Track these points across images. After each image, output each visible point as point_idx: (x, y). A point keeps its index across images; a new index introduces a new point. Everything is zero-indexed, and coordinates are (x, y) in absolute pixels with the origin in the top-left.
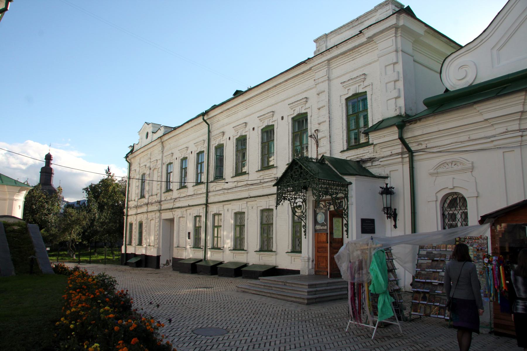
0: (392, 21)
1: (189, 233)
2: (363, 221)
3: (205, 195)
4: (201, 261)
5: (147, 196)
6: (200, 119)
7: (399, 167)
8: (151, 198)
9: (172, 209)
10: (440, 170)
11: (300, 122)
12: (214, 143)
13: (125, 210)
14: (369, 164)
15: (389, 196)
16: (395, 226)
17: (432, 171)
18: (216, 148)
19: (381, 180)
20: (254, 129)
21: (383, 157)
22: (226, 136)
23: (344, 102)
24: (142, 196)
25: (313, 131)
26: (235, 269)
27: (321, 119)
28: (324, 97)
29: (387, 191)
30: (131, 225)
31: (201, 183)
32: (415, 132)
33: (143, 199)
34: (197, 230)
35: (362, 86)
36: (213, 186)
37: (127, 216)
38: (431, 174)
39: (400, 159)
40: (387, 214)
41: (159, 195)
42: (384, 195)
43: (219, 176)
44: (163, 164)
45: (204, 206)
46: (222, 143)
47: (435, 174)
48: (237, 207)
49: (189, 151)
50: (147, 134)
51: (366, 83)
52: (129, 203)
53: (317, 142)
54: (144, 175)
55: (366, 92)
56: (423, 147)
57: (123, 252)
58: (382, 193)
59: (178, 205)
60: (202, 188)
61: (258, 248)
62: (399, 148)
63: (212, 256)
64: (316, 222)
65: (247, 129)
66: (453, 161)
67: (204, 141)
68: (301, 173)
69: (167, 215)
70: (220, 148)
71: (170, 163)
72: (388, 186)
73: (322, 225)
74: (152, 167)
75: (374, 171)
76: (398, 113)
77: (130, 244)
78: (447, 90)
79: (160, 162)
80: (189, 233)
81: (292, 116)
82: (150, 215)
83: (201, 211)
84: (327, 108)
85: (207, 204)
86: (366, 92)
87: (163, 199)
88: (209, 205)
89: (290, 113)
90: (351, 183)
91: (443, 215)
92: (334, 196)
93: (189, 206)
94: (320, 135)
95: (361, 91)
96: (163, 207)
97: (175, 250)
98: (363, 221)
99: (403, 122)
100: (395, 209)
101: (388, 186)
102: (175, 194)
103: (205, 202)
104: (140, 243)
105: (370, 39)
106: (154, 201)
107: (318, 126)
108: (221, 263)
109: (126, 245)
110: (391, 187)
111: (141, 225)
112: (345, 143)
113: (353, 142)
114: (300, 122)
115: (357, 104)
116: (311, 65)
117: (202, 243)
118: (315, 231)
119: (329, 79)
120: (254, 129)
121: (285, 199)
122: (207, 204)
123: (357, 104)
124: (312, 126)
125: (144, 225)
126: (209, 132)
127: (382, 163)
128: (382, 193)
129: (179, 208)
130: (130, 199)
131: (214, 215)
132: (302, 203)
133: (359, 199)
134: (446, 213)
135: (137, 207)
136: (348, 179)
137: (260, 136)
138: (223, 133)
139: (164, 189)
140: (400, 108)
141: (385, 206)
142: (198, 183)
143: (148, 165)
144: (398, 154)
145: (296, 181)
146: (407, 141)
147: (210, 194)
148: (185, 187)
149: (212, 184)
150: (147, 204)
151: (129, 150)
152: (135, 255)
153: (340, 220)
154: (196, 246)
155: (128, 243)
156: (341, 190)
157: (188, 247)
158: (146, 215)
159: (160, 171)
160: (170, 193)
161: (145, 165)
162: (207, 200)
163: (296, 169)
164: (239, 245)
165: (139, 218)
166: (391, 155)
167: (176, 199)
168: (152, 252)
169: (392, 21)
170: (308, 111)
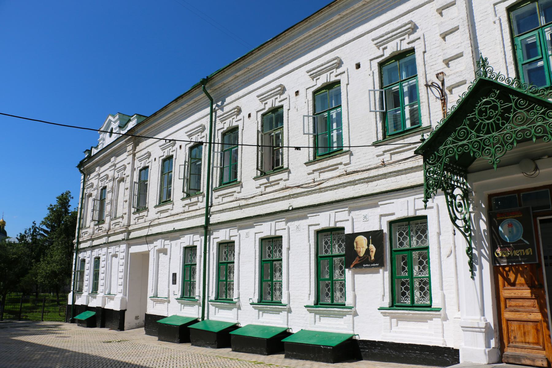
1: (174, 275)
4: (196, 321)
34: (189, 269)
41: (126, 217)
43: (230, 178)
44: (133, 169)
48: (266, 229)
57: (70, 302)
74: (116, 176)
79: (129, 168)
80: (174, 275)
81: (380, 60)
82: (112, 250)
93: (175, 231)
97: (150, 302)
102: (152, 213)
103: (204, 223)
108: (235, 327)
109: (74, 293)
117: (198, 291)
131: (220, 244)
132: (463, 199)
152: (85, 308)
154: (187, 294)
157: (172, 298)
158: (104, 250)
162: (207, 220)
165: (96, 253)
168: (114, 305)
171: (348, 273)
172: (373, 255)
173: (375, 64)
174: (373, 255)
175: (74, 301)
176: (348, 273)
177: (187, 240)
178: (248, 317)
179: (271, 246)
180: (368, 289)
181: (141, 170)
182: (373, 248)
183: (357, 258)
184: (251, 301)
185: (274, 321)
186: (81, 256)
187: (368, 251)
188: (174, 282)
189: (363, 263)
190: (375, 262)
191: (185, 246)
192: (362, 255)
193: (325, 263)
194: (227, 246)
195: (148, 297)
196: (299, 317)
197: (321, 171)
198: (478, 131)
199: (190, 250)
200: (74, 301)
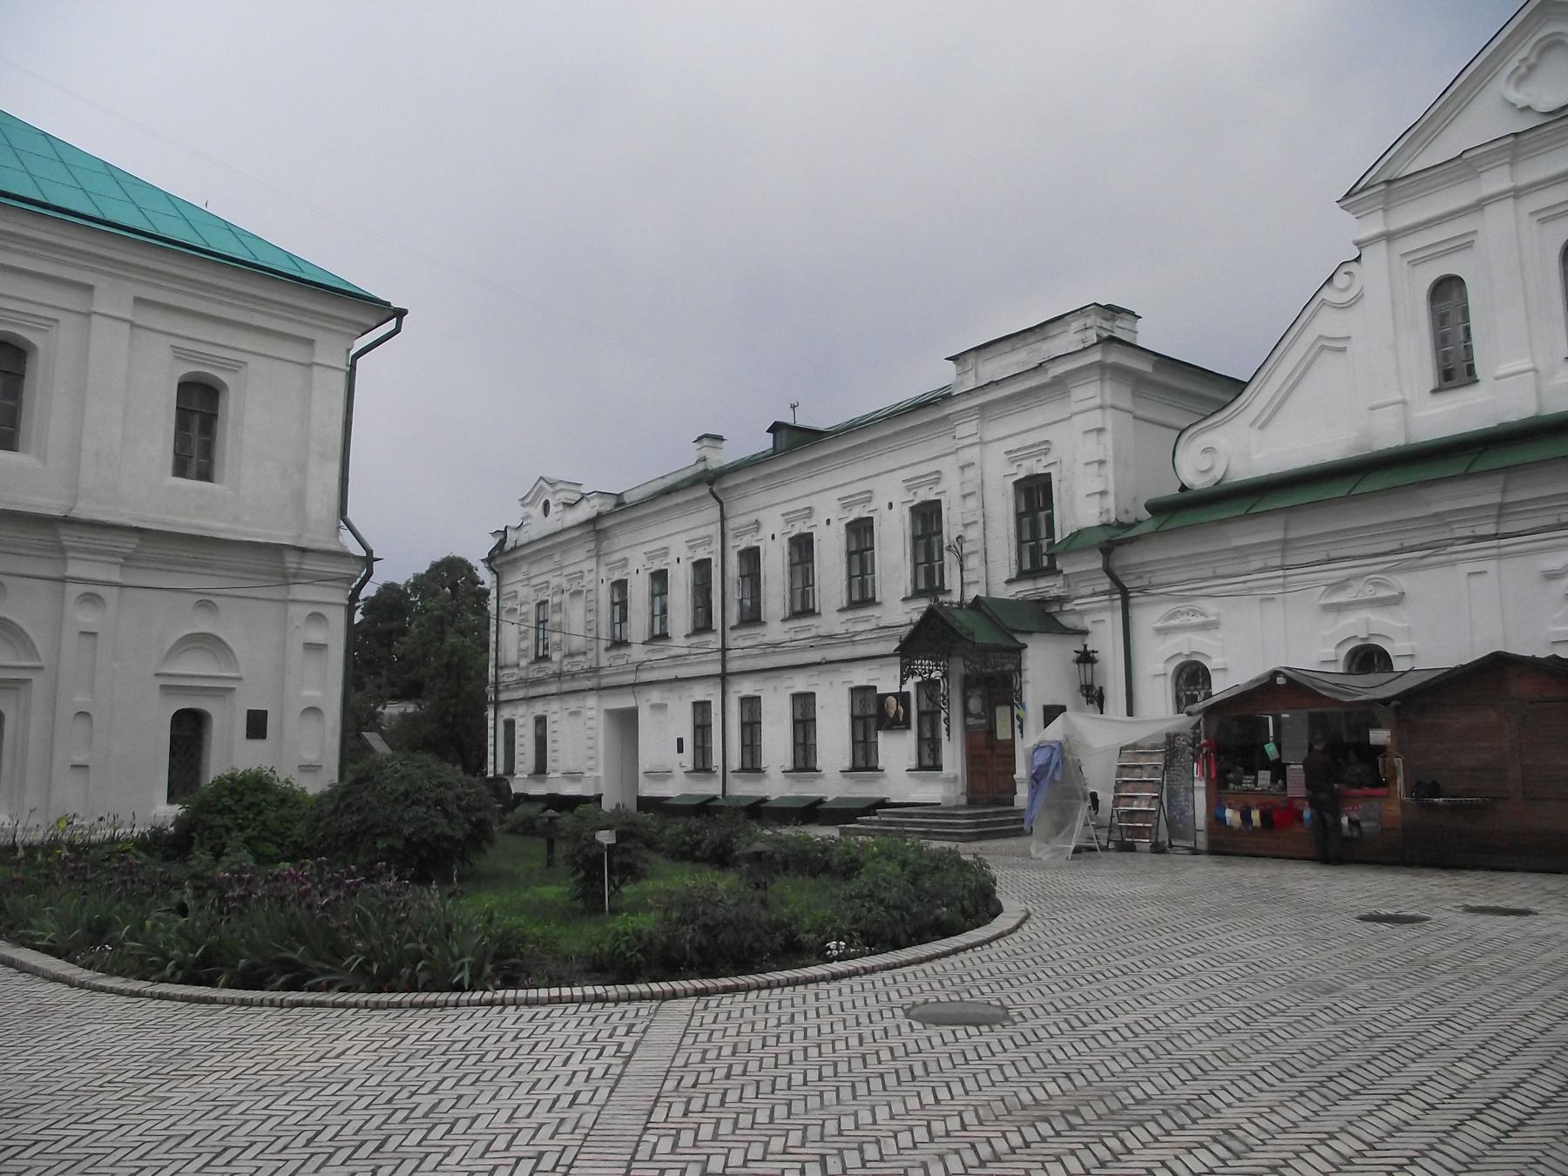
0: (1096, 356)
1: (680, 741)
3: (718, 656)
4: (714, 798)
5: (556, 656)
6: (704, 490)
7: (1106, 616)
8: (566, 662)
9: (634, 685)
10: (1173, 622)
11: (927, 517)
13: (490, 689)
14: (1055, 608)
17: (1158, 625)
18: (742, 554)
19: (1077, 638)
20: (828, 522)
23: (1011, 488)
25: (953, 538)
29: (1086, 658)
30: (510, 725)
32: (1130, 557)
34: (702, 729)
36: (737, 640)
40: (1087, 696)
43: (752, 617)
45: (719, 680)
47: (1163, 631)
48: (801, 683)
50: (547, 504)
52: (501, 673)
56: (1145, 582)
58: (1078, 661)
59: (646, 676)
61: (847, 764)
62: (1106, 584)
63: (744, 789)
64: (966, 713)
69: (623, 702)
70: (751, 557)
73: (978, 717)
75: (1066, 621)
76: (1105, 519)
78: (1183, 488)
80: (680, 741)
82: (573, 703)
84: (979, 494)
87: (604, 663)
88: (731, 678)
93: (677, 679)
95: (1041, 471)
96: (605, 682)
99: (1112, 541)
102: (637, 653)
104: (541, 769)
111: (541, 721)
112: (1014, 566)
114: (927, 517)
115: (1035, 495)
117: (716, 760)
118: (966, 728)
120: (828, 522)
123: (1035, 495)
124: (951, 525)
126: (723, 519)
128: (1078, 661)
129: (651, 683)
130: (502, 662)
131: (743, 700)
136: (1021, 639)
137: (844, 538)
140: (1108, 511)
143: (555, 582)
144: (1104, 593)
146: (1118, 573)
147: (730, 654)
149: (736, 633)
150: (559, 676)
151: (493, 542)
153: (1008, 709)
160: (623, 651)
164: (804, 759)
165: (539, 708)
166: (1094, 594)
167: (642, 663)
169: (1096, 356)
171: (881, 734)
173: (906, 508)
176: (881, 734)
177: (699, 693)
179: (804, 706)
180: (897, 750)
182: (901, 709)
186: (506, 713)
187: (897, 712)
188: (680, 750)
189: (898, 724)
193: (860, 724)
194: (751, 705)
195: (641, 775)
196: (833, 779)
197: (855, 621)
199: (702, 708)
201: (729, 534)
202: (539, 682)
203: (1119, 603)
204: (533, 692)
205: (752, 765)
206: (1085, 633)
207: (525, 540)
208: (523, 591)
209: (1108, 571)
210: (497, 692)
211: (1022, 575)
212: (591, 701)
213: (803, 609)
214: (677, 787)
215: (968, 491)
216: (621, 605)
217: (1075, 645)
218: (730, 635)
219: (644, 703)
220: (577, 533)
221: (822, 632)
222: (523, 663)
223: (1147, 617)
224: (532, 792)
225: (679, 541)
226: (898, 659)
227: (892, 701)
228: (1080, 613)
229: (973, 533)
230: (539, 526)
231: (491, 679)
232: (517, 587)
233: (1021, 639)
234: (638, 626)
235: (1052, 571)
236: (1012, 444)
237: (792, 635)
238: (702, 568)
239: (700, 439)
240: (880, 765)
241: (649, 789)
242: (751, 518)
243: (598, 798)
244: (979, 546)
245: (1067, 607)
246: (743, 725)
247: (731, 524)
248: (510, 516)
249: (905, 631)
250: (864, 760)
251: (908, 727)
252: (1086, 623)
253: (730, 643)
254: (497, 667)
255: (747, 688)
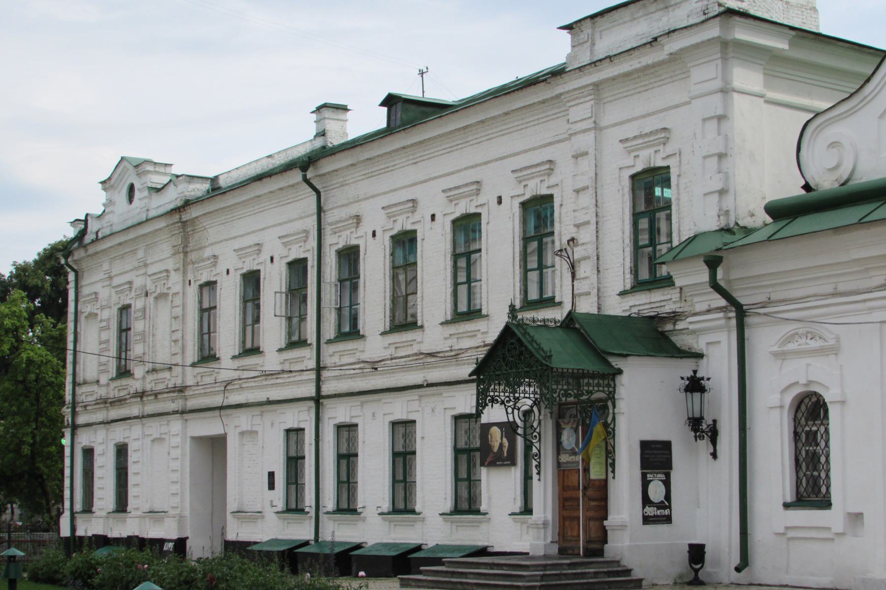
1: (271, 475)
2: (645, 445)
3: (313, 376)
4: (306, 543)
5: (139, 371)
6: (296, 176)
8: (150, 377)
9: (221, 408)
10: (791, 346)
11: (538, 212)
12: (334, 242)
13: (66, 411)
14: (669, 327)
15: (697, 395)
16: (714, 455)
17: (775, 349)
18: (340, 253)
20: (433, 217)
21: (695, 314)
22: (366, 228)
23: (627, 183)
24: (124, 372)
25: (565, 241)
26: (394, 557)
27: (582, 218)
28: (586, 166)
29: (695, 385)
30: (89, 453)
31: (302, 343)
33: (124, 382)
34: (294, 463)
35: (662, 155)
36: (333, 355)
37: (75, 428)
38: (776, 355)
39: (723, 322)
42: (688, 393)
45: (312, 404)
46: (354, 242)
47: (781, 356)
49: (265, 256)
50: (131, 188)
51: (670, 149)
52: (79, 390)
53: (573, 267)
54: (125, 309)
55: (668, 167)
59: (235, 398)
60: (306, 357)
61: (448, 506)
64: (559, 447)
65: (417, 217)
66: (808, 333)
67: (306, 232)
68: (521, 353)
69: (209, 427)
70: (350, 257)
71: (211, 285)
72: (699, 375)
73: (573, 453)
75: (681, 341)
77: (88, 508)
80: (271, 475)
81: (522, 199)
82: (155, 428)
83: (302, 417)
85: (318, 400)
86: (668, 167)
87: (190, 382)
88: (325, 402)
89: (516, 193)
90: (620, 372)
91: (796, 434)
92: (585, 397)
93: (269, 402)
94: (578, 253)
95: (660, 163)
96: (192, 404)
98: (645, 445)
100: (715, 421)
101: (699, 375)
103: (314, 394)
104: (122, 505)
105: (674, 57)
106: (160, 387)
107: (575, 229)
108: (359, 546)
110: (703, 379)
111: (122, 451)
112: (628, 276)
113: (644, 275)
114: (538, 212)
116: (559, 90)
118: (559, 464)
119: (597, 128)
120: (433, 217)
121: (493, 401)
122: (318, 400)
124: (563, 227)
125: (132, 457)
126: (320, 210)
127: (691, 327)
130: (80, 379)
131: (339, 427)
133: (644, 401)
134: (799, 430)
135: (105, 402)
137: (449, 237)
138: (358, 219)
139: (192, 355)
140: (727, 213)
141: (691, 416)
142: (295, 343)
143: (138, 282)
145: (511, 369)
147: (325, 374)
148: (255, 351)
149: (332, 348)
152: (102, 541)
155: (78, 507)
156: (598, 385)
159: (178, 301)
161: (130, 283)
162: (318, 388)
163: (512, 344)
165: (119, 434)
166: (709, 311)
167: (229, 383)
168: (166, 531)
169: (713, 31)
170: (555, 192)
171: (484, 471)
172: (505, 450)
173: (516, 203)
174: (505, 450)
175: (73, 529)
178: (373, 531)
181: (201, 287)
182: (505, 440)
183: (491, 454)
184: (380, 511)
185: (404, 534)
186: (84, 439)
187: (501, 445)
188: (271, 486)
189: (504, 460)
190: (507, 459)
191: (287, 427)
192: (495, 450)
193: (464, 458)
194: (347, 430)
195: (228, 513)
196: (433, 527)
197: (459, 336)
198: (506, 365)
199: (294, 434)
200: (73, 529)
201: (327, 230)
202: (119, 402)
203: (734, 322)
204: (114, 413)
205: (347, 507)
206: (700, 356)
207: (107, 231)
208: (104, 293)
209: (715, 286)
210: (74, 414)
211: (639, 286)
212: (176, 425)
213: (403, 321)
214: (270, 529)
215: (580, 185)
216: (207, 312)
217: (685, 368)
218: (327, 350)
219: (233, 427)
220: (161, 224)
221: (425, 349)
222: (104, 380)
223: (764, 339)
224: (114, 534)
225: (274, 234)
226: (474, 386)
227: (496, 432)
228: (694, 332)
229: (586, 235)
230: (124, 213)
231: (68, 398)
232: (98, 288)
233: (616, 362)
234: (227, 340)
235: (668, 282)
236: (629, 131)
237: (391, 351)
238: (297, 267)
239: (319, 109)
240: (483, 508)
241: (237, 532)
242: (353, 210)
243: (181, 544)
244: (591, 250)
245: (680, 325)
246: (340, 457)
247: (330, 217)
248: (94, 202)
249: (481, 354)
250: (466, 504)
251: (514, 463)
252: (699, 344)
253: (327, 360)
254: (75, 384)
255: (338, 413)
